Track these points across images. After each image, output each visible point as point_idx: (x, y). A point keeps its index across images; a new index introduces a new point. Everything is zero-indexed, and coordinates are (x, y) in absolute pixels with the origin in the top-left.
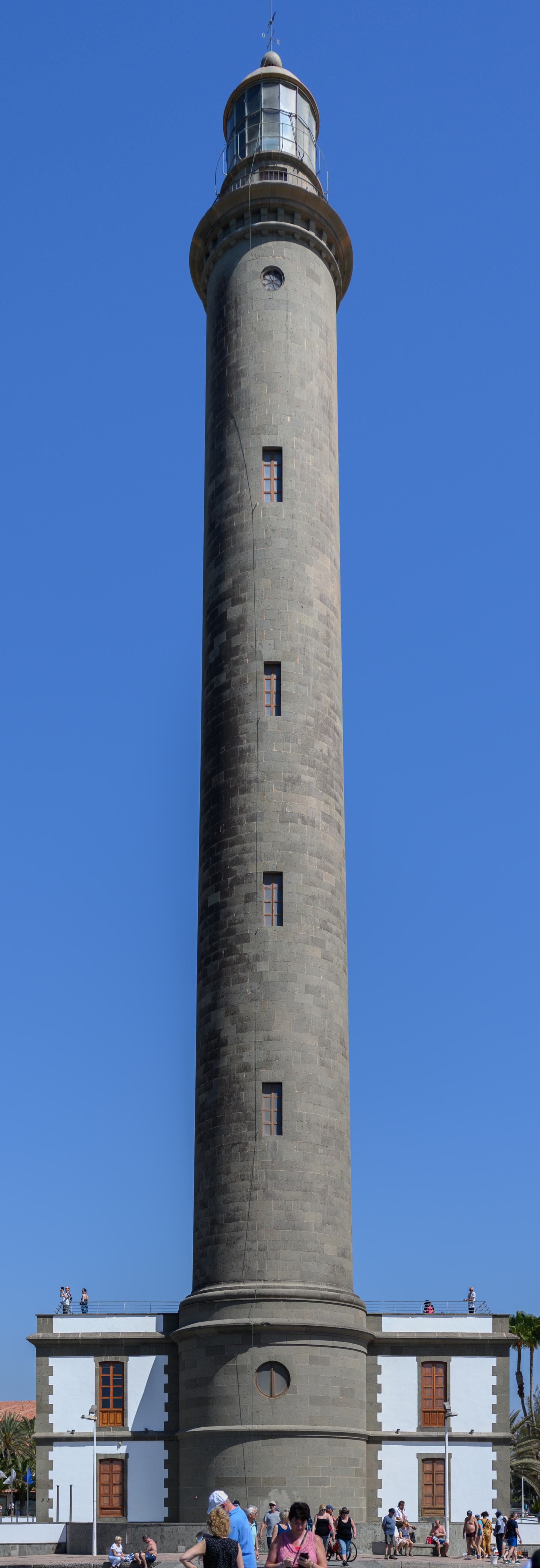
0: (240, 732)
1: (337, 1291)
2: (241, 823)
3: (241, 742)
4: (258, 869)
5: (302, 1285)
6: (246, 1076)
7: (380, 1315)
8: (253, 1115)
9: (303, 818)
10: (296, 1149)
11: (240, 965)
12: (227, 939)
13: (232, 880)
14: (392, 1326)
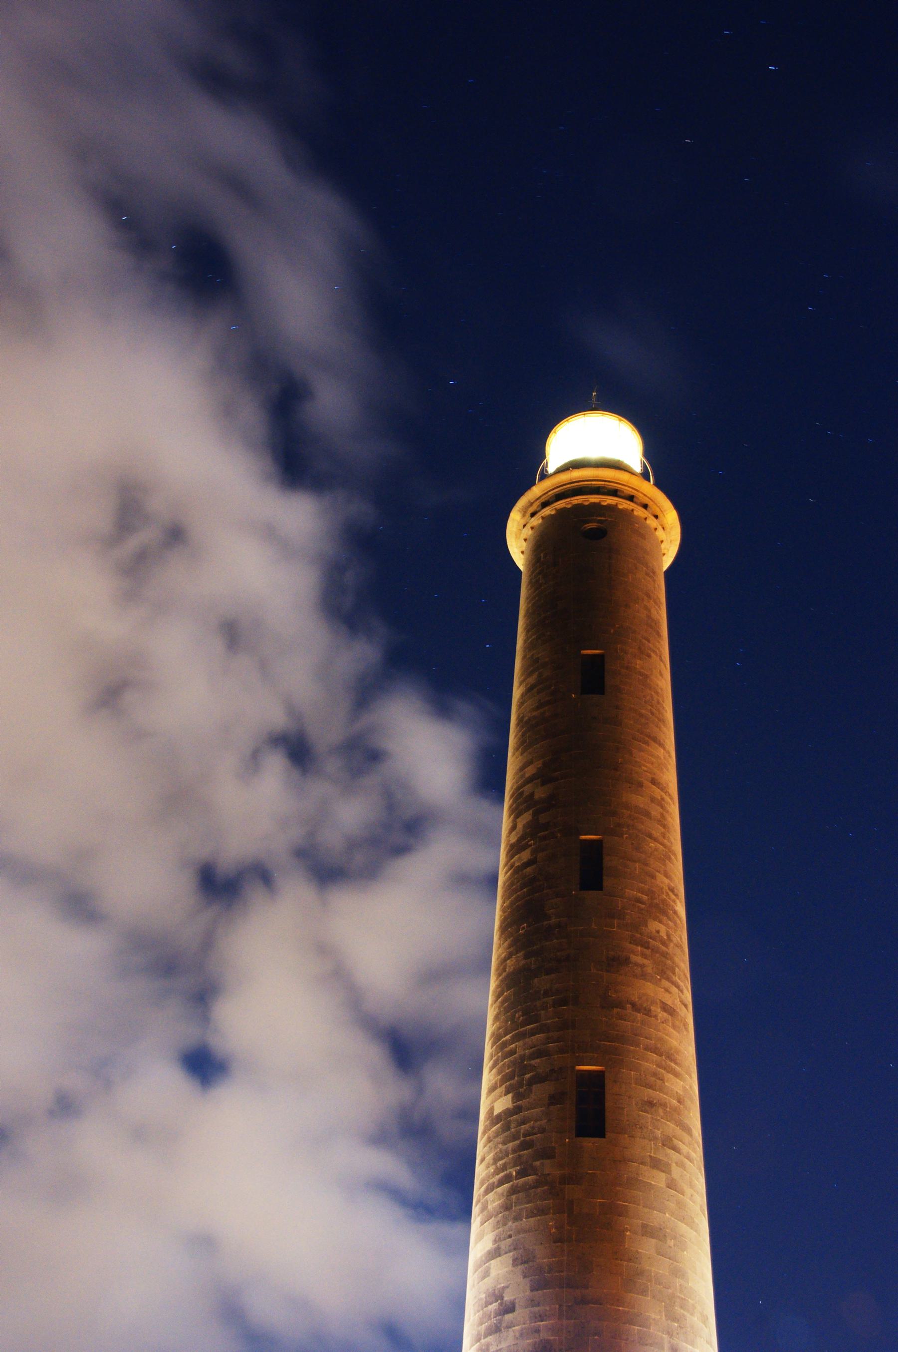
12: (519, 1155)
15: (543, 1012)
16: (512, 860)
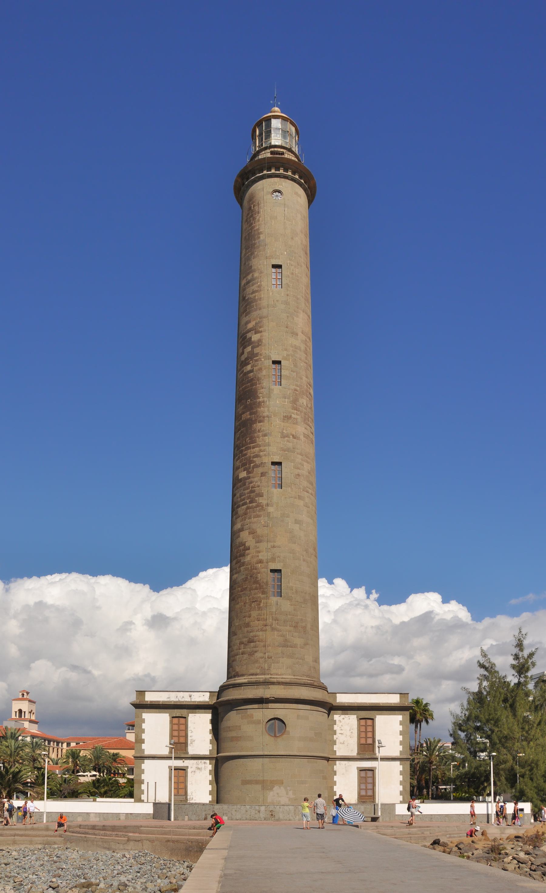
0: (258, 393)
1: (312, 681)
2: (259, 437)
3: (259, 398)
4: (267, 460)
5: (293, 677)
6: (261, 566)
7: (336, 693)
8: (265, 586)
9: (293, 436)
10: (289, 605)
11: (258, 508)
13: (253, 465)
14: (342, 699)
15: (257, 439)
16: (243, 369)
